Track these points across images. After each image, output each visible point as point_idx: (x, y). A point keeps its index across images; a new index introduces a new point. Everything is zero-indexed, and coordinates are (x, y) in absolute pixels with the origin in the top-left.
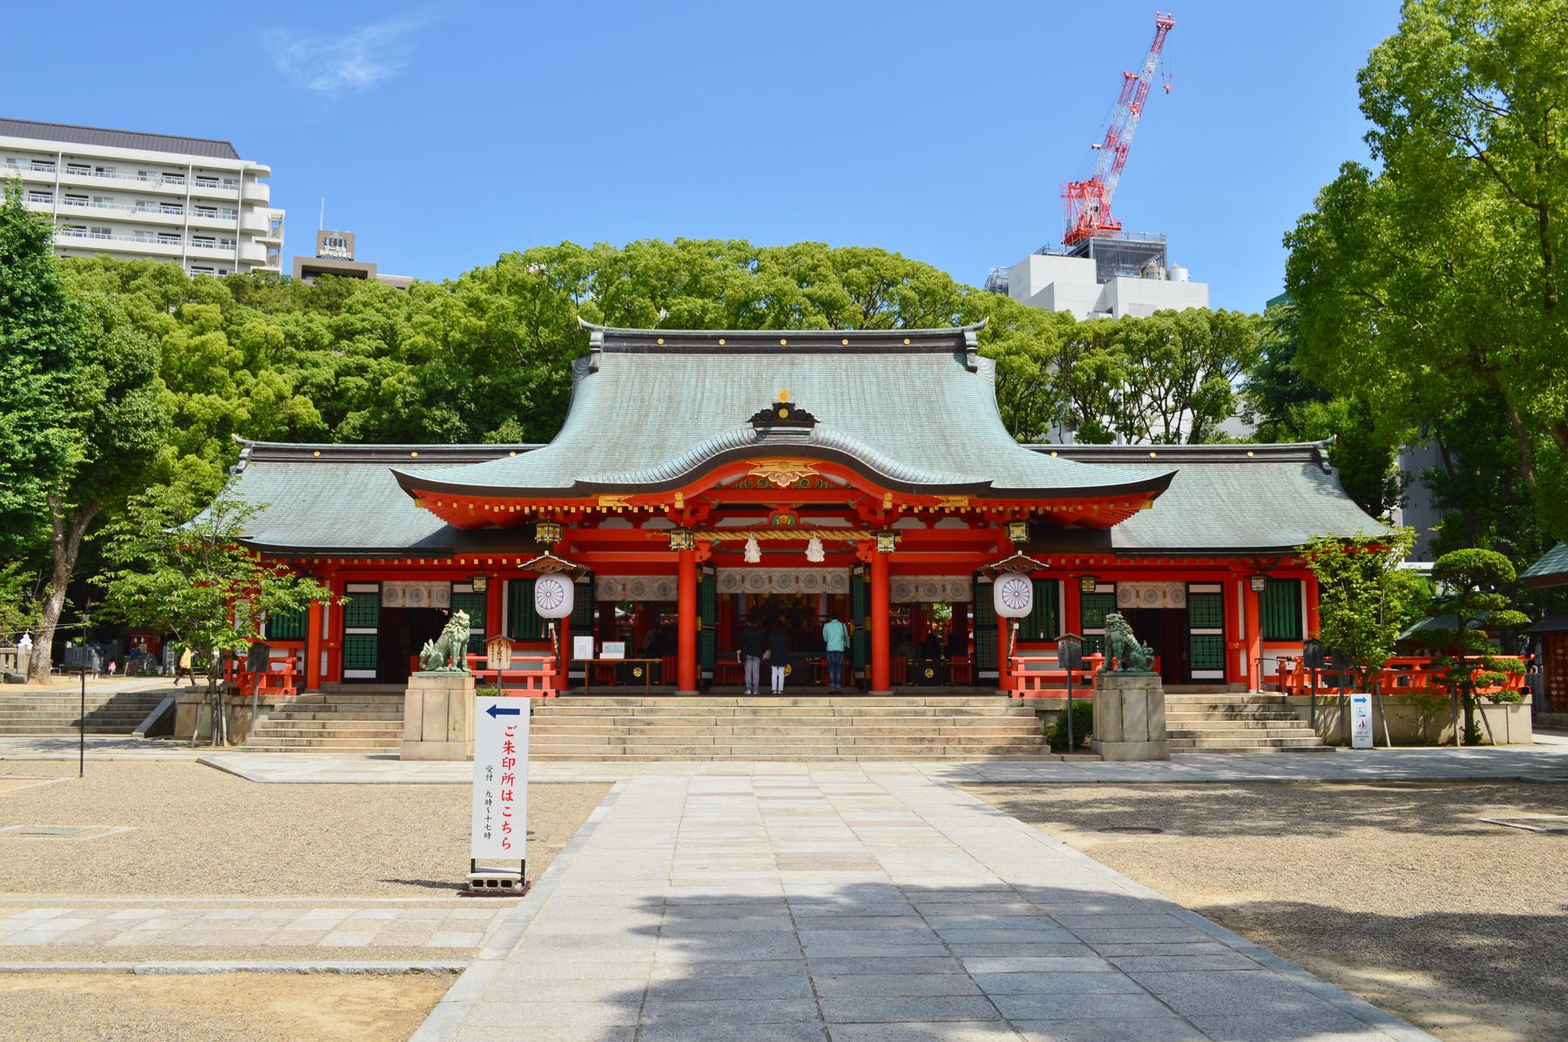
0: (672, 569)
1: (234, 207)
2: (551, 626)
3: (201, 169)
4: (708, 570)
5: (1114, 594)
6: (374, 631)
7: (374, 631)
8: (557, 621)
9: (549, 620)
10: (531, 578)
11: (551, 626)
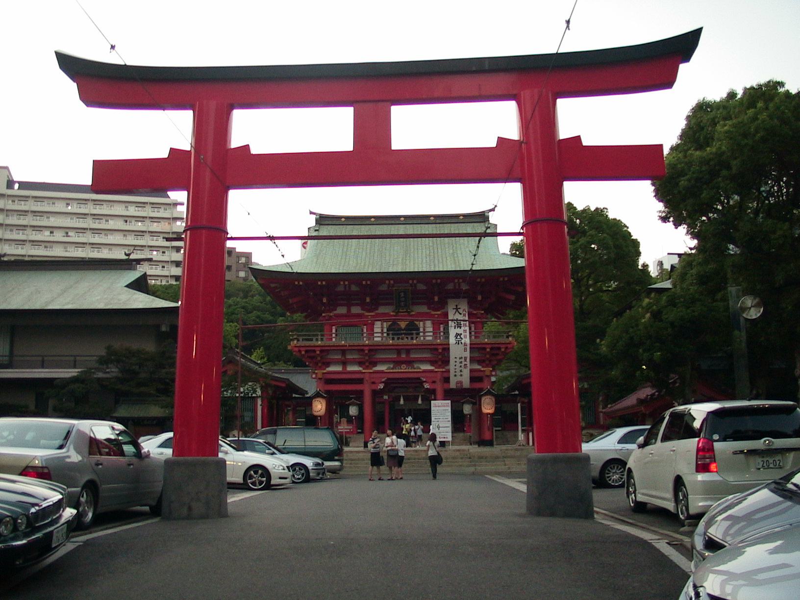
0: (383, 403)
1: (168, 221)
2: (354, 418)
3: (153, 204)
4: (391, 403)
5: (501, 407)
6: (304, 420)
7: (304, 420)
8: (355, 416)
9: (353, 416)
10: (348, 406)
11: (354, 418)
